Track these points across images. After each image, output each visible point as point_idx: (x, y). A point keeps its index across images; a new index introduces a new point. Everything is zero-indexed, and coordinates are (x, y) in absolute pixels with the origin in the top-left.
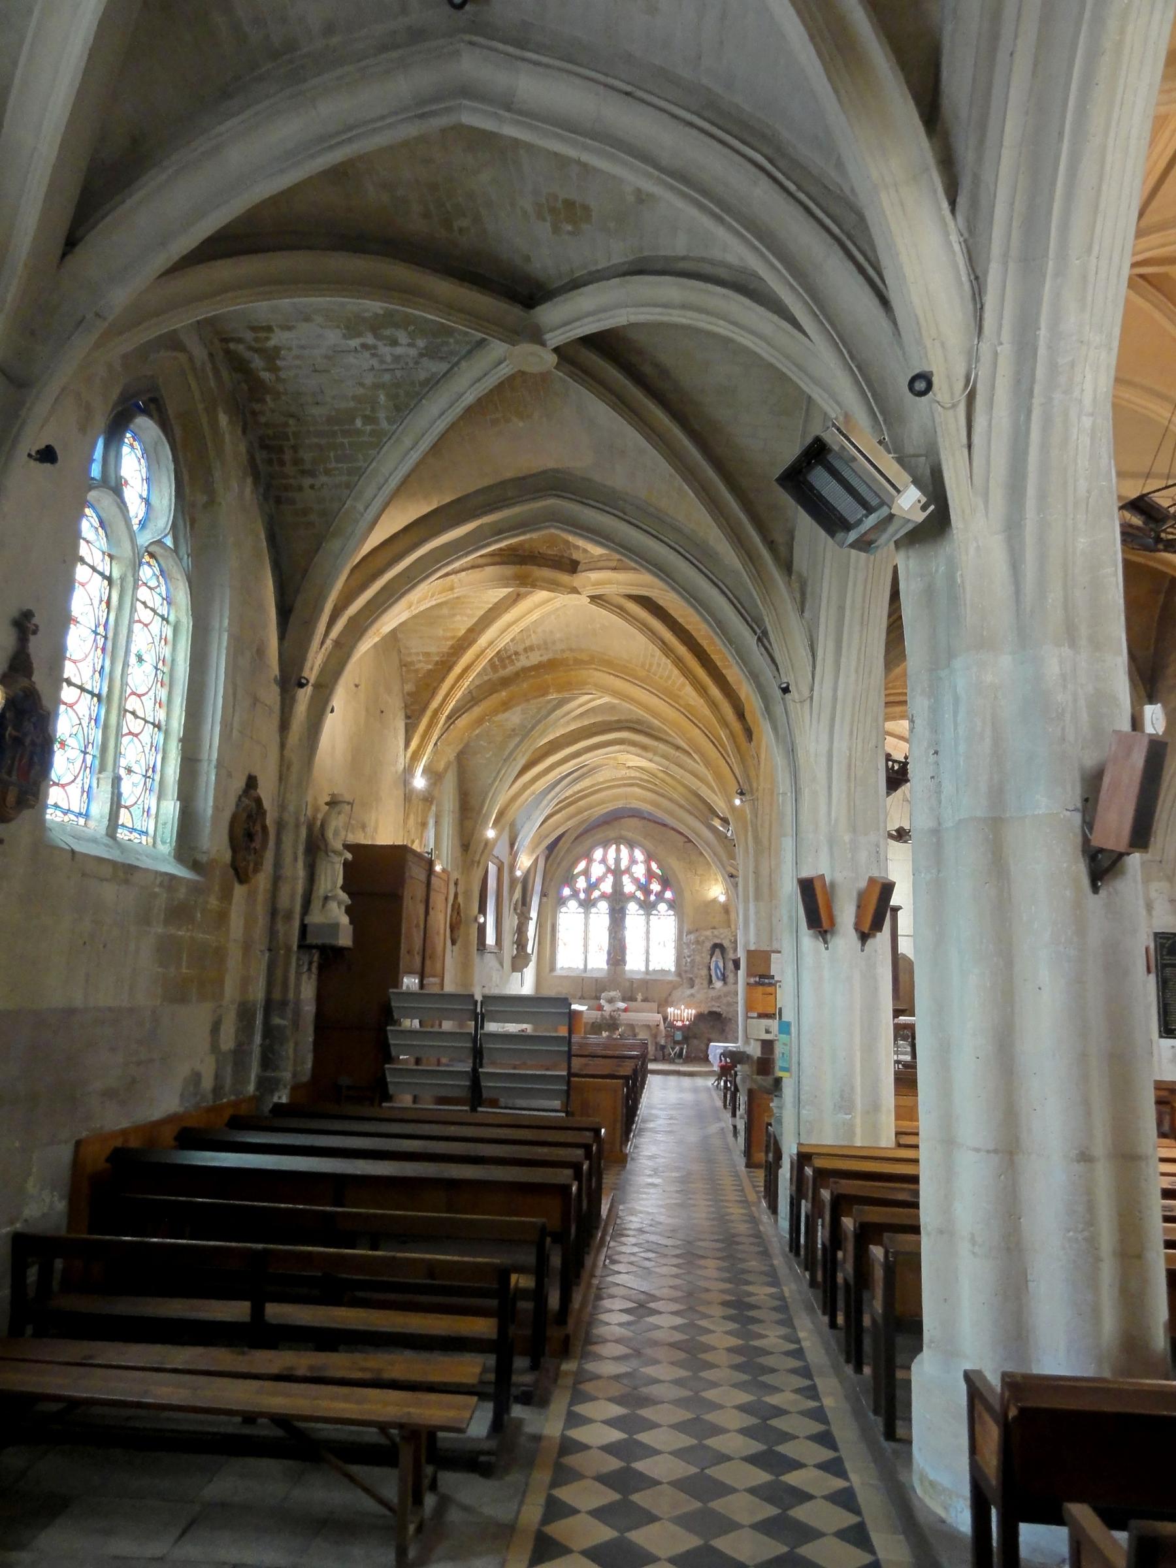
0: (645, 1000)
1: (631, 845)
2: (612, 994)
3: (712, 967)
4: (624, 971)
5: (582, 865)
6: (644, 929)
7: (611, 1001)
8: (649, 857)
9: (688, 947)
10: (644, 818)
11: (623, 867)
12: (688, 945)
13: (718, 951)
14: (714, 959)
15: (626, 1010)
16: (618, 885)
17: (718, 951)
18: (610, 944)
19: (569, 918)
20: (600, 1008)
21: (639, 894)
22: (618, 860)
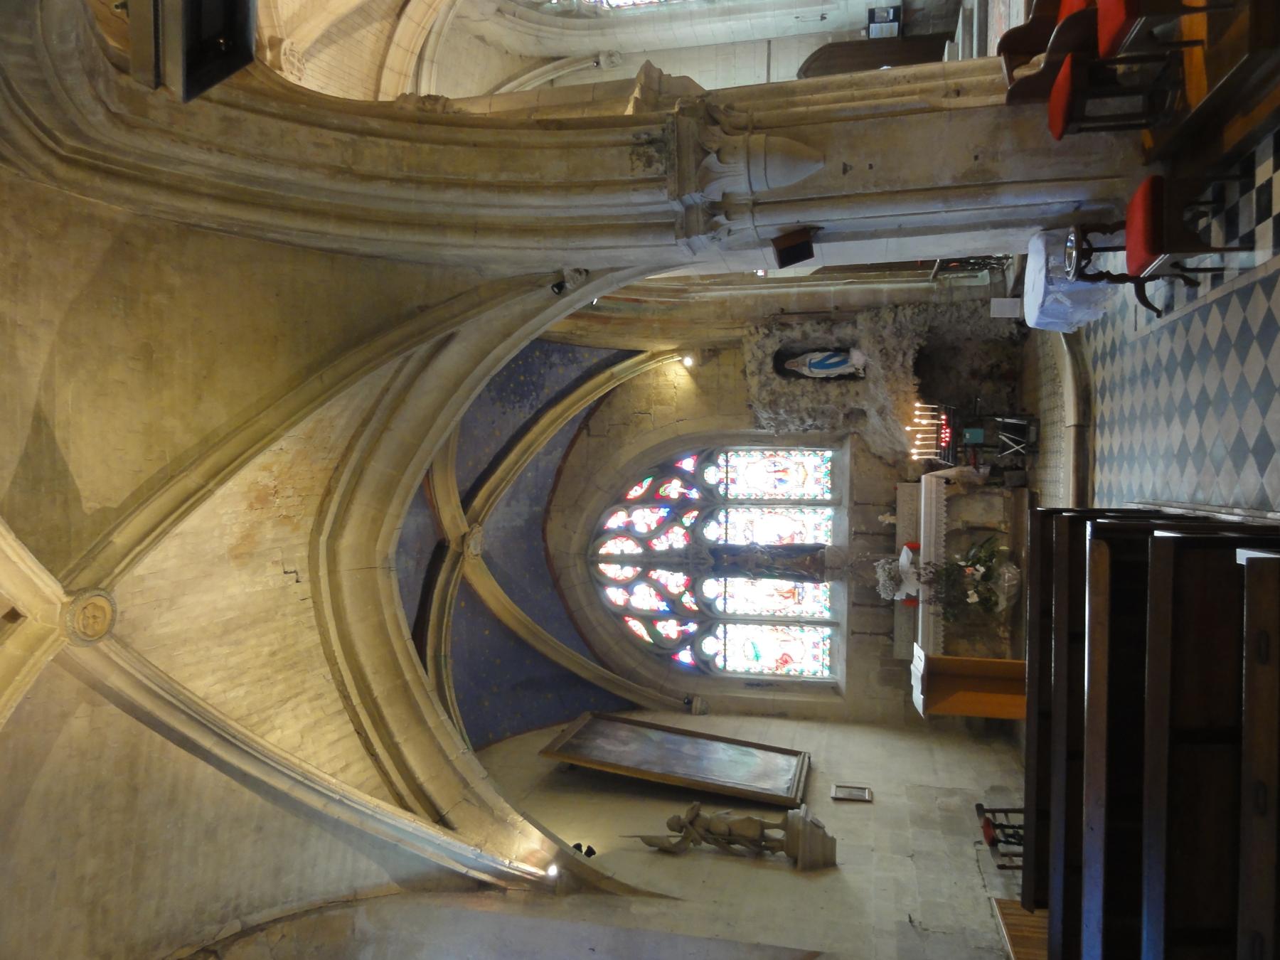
0: (892, 508)
1: (600, 534)
2: (881, 576)
3: (821, 373)
4: (835, 549)
5: (637, 627)
6: (755, 511)
7: (897, 580)
8: (620, 501)
9: (784, 423)
10: (547, 511)
11: (639, 550)
12: (780, 424)
13: (790, 365)
14: (806, 371)
15: (915, 548)
16: (672, 561)
17: (790, 365)
18: (782, 576)
19: (740, 652)
20: (912, 601)
21: (688, 520)
22: (623, 560)
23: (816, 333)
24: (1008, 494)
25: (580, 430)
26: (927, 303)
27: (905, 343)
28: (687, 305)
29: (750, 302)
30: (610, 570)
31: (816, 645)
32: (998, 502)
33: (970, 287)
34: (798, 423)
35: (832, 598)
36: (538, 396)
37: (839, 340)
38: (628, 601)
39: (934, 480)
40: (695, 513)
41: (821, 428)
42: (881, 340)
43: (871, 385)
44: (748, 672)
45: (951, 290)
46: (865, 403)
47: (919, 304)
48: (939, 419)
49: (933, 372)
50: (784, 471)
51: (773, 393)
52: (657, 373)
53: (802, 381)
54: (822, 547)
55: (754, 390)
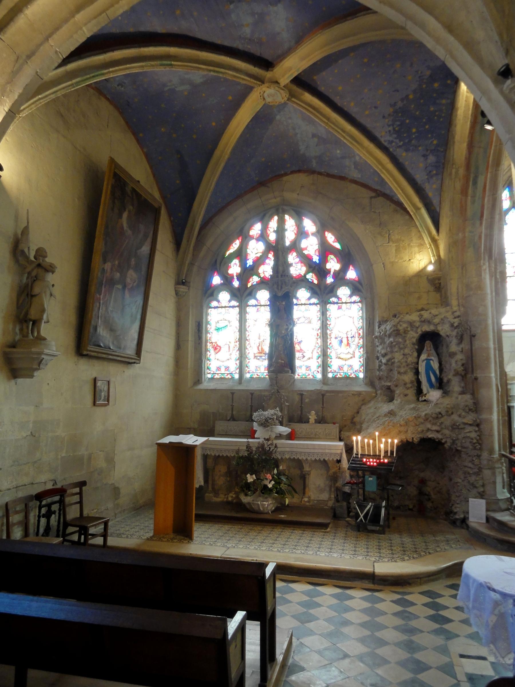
0: (321, 420)
2: (269, 413)
3: (422, 368)
5: (236, 245)
7: (266, 424)
8: (323, 227)
9: (383, 342)
10: (313, 172)
11: (288, 243)
12: (381, 338)
13: (428, 344)
14: (423, 357)
16: (281, 268)
17: (428, 344)
19: (221, 318)
20: (252, 434)
21: (311, 276)
23: (455, 364)
24: (330, 504)
25: (375, 191)
26: (480, 449)
27: (447, 432)
28: (478, 258)
29: (481, 310)
30: (273, 224)
31: (227, 368)
32: (325, 496)
33: (494, 483)
34: (383, 352)
35: (259, 379)
36: (400, 147)
37: (449, 381)
38: (252, 237)
39: (339, 452)
40: (316, 282)
41: (380, 370)
42: (449, 413)
43: (413, 406)
44: (207, 323)
45: (492, 469)
46: (399, 400)
47: (480, 444)
48: (385, 457)
49: (423, 453)
50: (348, 344)
51: (406, 332)
52: (421, 245)
53: (415, 354)
54: (293, 371)
55: (408, 318)
